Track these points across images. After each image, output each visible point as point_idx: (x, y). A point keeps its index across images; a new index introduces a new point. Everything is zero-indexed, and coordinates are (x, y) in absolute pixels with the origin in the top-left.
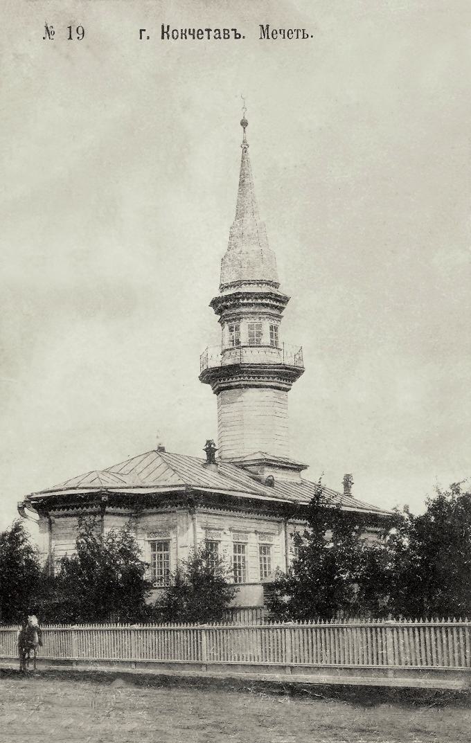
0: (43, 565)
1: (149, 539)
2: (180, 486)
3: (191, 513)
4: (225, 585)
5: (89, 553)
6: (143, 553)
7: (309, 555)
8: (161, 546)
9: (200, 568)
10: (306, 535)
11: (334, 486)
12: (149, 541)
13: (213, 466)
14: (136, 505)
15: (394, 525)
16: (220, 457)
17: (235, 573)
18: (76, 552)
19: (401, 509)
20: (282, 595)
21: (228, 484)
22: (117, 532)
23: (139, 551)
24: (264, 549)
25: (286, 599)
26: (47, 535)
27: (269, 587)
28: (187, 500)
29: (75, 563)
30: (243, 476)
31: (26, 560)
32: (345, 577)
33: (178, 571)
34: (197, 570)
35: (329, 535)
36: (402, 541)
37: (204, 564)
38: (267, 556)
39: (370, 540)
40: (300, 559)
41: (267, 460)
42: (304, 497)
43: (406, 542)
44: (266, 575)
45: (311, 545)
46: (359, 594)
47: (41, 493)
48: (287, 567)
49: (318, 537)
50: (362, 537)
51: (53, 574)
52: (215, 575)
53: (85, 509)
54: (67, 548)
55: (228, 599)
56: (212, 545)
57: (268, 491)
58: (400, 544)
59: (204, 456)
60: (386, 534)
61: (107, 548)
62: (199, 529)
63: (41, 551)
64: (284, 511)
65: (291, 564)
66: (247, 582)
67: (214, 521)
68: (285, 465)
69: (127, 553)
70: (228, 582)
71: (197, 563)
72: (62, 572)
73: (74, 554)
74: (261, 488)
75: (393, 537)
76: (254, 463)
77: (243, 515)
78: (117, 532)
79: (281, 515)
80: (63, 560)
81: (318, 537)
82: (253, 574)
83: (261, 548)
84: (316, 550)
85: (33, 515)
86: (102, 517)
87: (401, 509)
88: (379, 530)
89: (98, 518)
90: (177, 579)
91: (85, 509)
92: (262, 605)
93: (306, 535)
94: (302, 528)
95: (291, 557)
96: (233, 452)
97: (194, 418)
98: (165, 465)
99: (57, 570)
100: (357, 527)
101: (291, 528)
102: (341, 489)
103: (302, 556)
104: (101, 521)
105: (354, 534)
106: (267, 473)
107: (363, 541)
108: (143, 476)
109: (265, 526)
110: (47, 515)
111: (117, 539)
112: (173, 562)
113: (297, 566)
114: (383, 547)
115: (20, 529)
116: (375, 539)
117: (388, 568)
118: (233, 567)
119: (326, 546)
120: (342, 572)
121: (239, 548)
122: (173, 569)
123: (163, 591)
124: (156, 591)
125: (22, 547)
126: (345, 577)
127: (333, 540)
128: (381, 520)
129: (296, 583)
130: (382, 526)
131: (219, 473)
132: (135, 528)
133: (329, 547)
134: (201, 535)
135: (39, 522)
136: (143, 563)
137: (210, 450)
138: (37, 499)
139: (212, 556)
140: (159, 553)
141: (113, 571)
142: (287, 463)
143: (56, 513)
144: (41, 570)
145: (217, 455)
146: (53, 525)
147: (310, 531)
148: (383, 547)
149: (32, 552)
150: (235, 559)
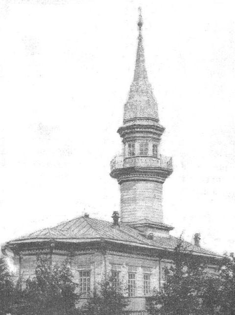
0: (15, 284)
1: (79, 269)
2: (97, 238)
3: (104, 254)
4: (124, 298)
5: (42, 277)
6: (75, 278)
7: (172, 280)
8: (86, 274)
9: (108, 287)
10: (172, 269)
11: (189, 238)
12: (78, 271)
13: (117, 227)
14: (71, 249)
15: (224, 264)
16: (121, 222)
17: (129, 291)
18: (35, 276)
19: (229, 254)
20: (156, 304)
21: (126, 237)
22: (59, 264)
23: (73, 277)
24: (146, 277)
25: (159, 306)
26: (18, 266)
27: (149, 300)
28: (102, 247)
29: (34, 283)
30: (134, 233)
31: (5, 280)
32: (194, 294)
33: (95, 289)
34: (106, 288)
35: (185, 269)
36: (229, 273)
37: (111, 285)
38: (148, 281)
39: (209, 272)
40: (168, 283)
41: (149, 224)
42: (171, 247)
43: (231, 274)
44: (147, 292)
45: (174, 275)
46: (203, 304)
47: (16, 240)
48: (160, 287)
49: (178, 270)
50: (205, 271)
51: (21, 289)
52: (117, 291)
53: (41, 251)
54: (30, 275)
55: (125, 306)
56: (115, 274)
57: (149, 242)
58: (227, 275)
59: (111, 220)
60: (219, 269)
61: (53, 274)
62: (107, 263)
63: (15, 275)
64: (160, 255)
65: (162, 285)
66: (136, 295)
67: (116, 259)
68: (160, 227)
69: (66, 277)
70: (125, 295)
71: (107, 284)
72: (27, 288)
73: (34, 278)
74: (146, 241)
75: (223, 271)
76: (141, 225)
77: (135, 256)
78: (59, 264)
79: (157, 256)
80: (27, 280)
81: (178, 270)
82: (139, 292)
83: (144, 276)
84: (177, 278)
85: (11, 254)
86: (51, 255)
87: (229, 254)
88: (215, 266)
89: (49, 256)
90: (95, 293)
91: (41, 251)
92: (144, 309)
93: (172, 269)
94: (169, 264)
95: (162, 282)
96: (129, 219)
97: (103, 200)
98: (89, 225)
99: (24, 287)
100: (202, 265)
101: (163, 265)
102: (193, 243)
103: (169, 281)
104: (50, 258)
105: (200, 269)
106: (149, 232)
107: (206, 273)
108: (76, 231)
109: (147, 263)
110: (18, 254)
111: (59, 269)
112: (92, 283)
113: (166, 287)
114: (217, 277)
115: (3, 263)
116: (213, 272)
117: (220, 289)
118: (127, 287)
119: (183, 276)
120: (194, 291)
121: (131, 276)
122: (92, 287)
123: (86, 300)
124: (82, 300)
125: (4, 273)
126: (194, 294)
127: (188, 272)
128: (217, 260)
129: (166, 297)
130: (217, 264)
131: (121, 231)
132: (70, 263)
133: (185, 276)
134: (109, 268)
135: (14, 258)
136: (74, 284)
137: (115, 216)
138: (13, 244)
139: (116, 280)
140: (84, 277)
141: (56, 288)
142: (162, 226)
143: (23, 253)
144: (14, 287)
145: (119, 220)
146: (22, 260)
147: (174, 266)
148: (217, 277)
149: (9, 276)
150: (129, 282)
